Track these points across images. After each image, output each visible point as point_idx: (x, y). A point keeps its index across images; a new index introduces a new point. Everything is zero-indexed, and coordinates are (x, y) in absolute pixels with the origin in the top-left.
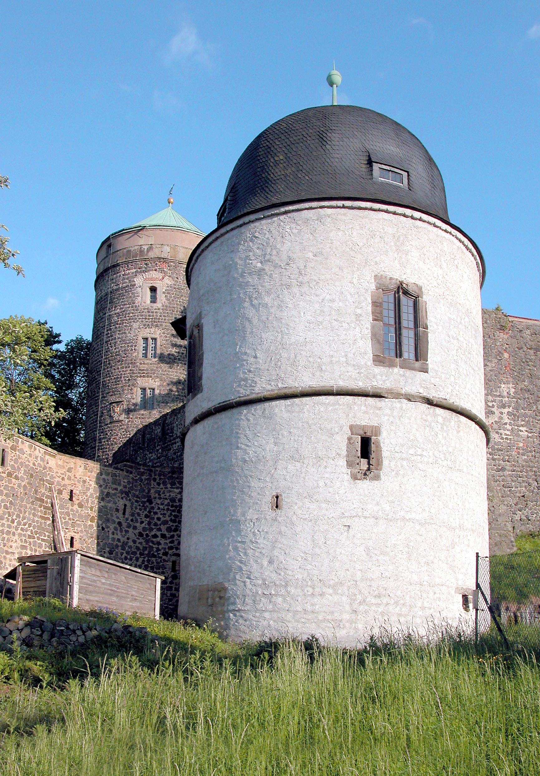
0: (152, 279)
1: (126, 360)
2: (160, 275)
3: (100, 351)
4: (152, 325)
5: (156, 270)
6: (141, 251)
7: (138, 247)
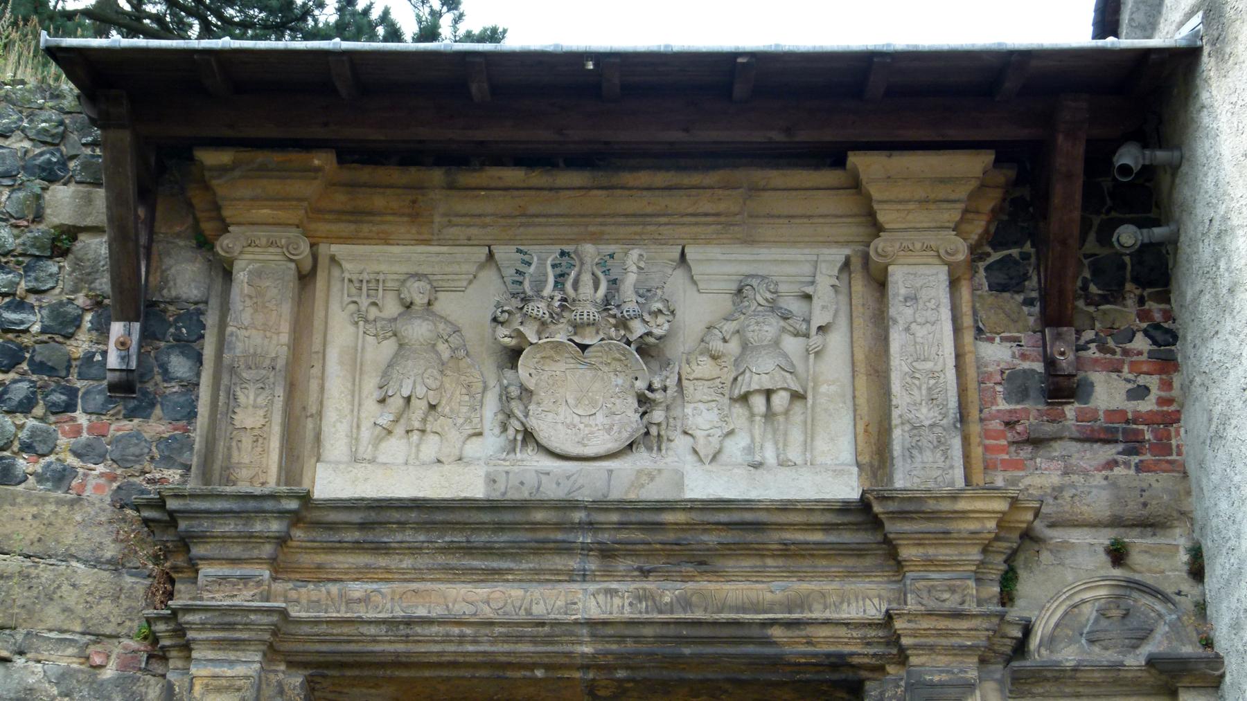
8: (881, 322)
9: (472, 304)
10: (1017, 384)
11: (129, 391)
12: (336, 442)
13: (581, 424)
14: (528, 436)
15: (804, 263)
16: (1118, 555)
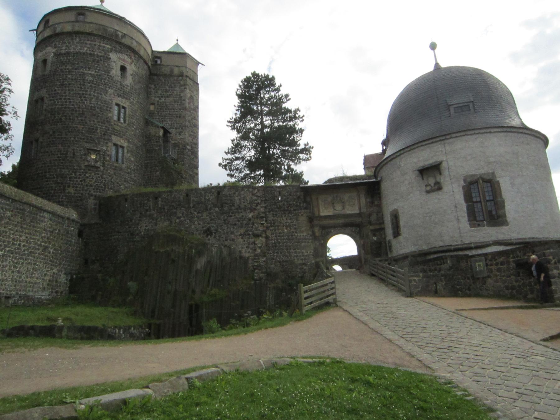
0: (124, 60)
2: (129, 60)
3: (69, 99)
5: (127, 55)
6: (117, 36)
8: (360, 199)
9: (330, 199)
11: (306, 208)
12: (321, 211)
13: (339, 208)
15: (354, 194)
16: (377, 215)
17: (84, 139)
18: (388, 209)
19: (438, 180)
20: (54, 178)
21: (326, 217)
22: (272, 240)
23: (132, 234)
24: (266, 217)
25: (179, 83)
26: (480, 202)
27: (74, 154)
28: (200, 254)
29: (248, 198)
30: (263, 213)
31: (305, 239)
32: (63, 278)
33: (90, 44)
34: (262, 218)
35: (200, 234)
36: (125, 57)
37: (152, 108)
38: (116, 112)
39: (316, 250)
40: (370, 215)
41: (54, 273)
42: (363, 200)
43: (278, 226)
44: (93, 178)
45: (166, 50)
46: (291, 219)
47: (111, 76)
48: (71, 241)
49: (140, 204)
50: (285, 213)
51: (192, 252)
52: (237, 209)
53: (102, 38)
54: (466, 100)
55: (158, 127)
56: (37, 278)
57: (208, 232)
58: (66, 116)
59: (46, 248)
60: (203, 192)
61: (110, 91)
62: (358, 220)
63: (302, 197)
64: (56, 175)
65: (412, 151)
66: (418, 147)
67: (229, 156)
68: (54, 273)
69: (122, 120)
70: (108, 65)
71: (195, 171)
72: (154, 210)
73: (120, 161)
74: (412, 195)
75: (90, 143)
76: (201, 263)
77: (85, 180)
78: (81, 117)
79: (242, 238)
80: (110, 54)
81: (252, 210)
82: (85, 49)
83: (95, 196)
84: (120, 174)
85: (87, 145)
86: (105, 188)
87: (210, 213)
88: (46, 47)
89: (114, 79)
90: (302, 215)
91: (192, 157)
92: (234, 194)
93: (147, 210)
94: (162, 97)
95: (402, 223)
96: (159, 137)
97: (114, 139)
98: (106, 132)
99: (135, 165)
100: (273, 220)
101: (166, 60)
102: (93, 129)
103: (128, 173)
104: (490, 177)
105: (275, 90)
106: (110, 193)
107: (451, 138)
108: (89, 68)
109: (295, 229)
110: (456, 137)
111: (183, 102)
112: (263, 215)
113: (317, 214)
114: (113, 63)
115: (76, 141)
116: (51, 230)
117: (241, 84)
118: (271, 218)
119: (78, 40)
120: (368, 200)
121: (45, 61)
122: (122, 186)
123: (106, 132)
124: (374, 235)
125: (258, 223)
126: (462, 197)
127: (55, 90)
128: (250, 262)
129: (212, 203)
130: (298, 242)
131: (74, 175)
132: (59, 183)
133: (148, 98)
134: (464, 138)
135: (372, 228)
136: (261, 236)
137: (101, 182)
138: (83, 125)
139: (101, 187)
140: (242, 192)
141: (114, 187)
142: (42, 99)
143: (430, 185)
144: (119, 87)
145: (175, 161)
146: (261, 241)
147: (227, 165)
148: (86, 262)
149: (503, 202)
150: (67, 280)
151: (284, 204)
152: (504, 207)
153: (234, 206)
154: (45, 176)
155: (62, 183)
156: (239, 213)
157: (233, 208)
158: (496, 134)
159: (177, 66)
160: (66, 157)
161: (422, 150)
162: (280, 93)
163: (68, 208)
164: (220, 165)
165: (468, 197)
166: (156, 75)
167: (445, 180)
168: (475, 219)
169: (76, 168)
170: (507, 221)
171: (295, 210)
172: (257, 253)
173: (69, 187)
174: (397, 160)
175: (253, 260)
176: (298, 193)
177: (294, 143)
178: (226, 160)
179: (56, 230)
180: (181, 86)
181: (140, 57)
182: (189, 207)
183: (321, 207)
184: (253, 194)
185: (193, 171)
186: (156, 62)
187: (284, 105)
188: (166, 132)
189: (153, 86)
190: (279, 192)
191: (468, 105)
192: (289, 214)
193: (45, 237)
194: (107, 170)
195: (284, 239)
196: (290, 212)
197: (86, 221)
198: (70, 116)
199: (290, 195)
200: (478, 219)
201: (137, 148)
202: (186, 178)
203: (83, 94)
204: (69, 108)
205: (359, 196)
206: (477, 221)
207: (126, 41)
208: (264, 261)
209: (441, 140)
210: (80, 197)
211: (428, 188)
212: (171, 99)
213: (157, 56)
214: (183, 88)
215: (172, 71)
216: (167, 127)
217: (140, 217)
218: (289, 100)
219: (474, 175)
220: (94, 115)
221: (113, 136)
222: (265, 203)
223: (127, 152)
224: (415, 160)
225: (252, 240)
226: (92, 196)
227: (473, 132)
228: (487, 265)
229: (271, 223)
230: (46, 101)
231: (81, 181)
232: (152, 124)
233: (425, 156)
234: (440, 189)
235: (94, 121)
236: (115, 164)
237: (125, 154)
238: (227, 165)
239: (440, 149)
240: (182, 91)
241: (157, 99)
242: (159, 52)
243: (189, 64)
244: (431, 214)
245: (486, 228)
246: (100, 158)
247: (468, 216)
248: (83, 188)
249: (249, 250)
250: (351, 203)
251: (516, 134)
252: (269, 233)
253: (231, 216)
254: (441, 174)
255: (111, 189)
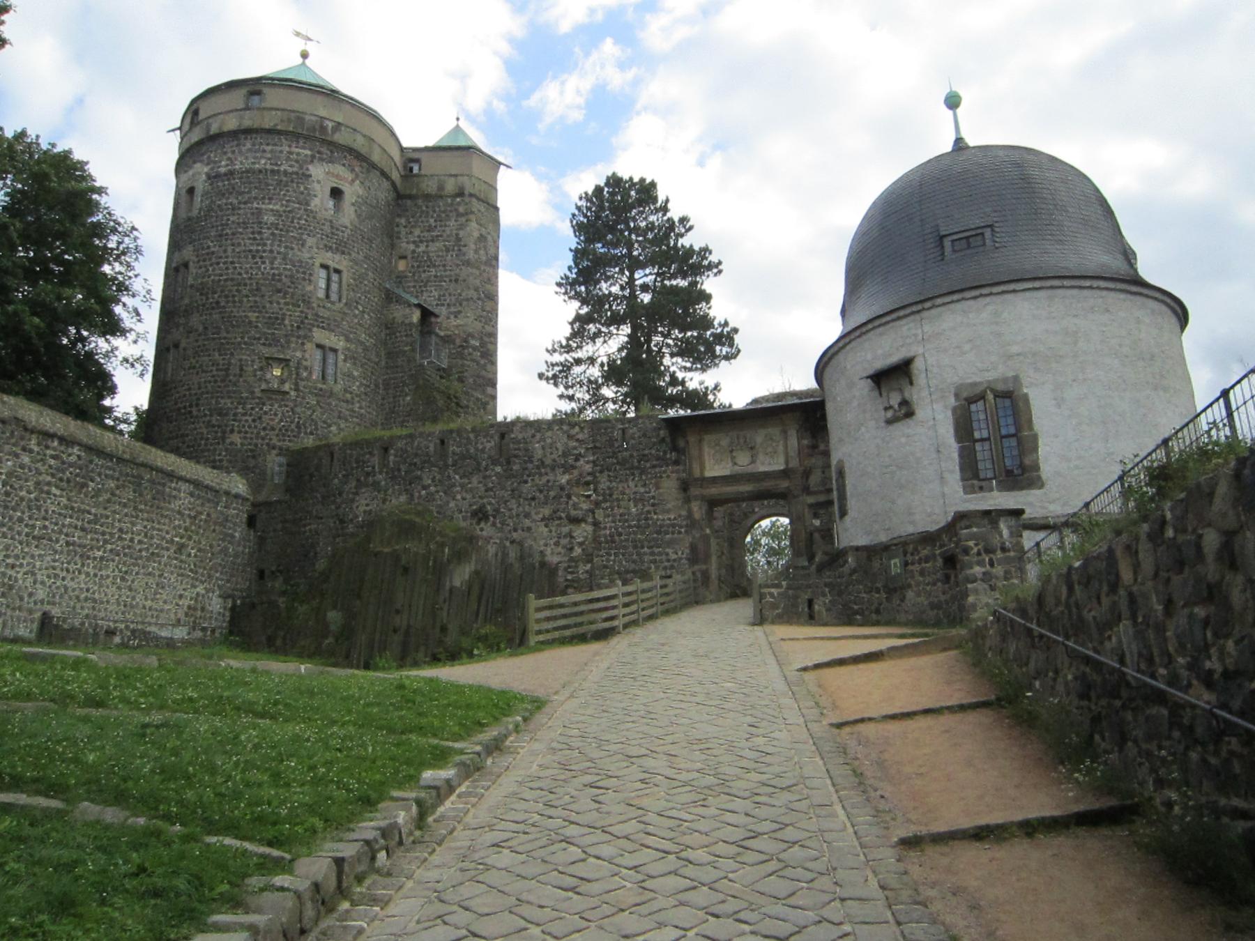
0: (337, 176)
1: (293, 294)
2: (350, 176)
3: (232, 263)
4: (337, 249)
6: (323, 129)
7: (313, 118)
8: (786, 439)
10: (808, 447)
11: (676, 462)
14: (735, 464)
15: (775, 431)
17: (259, 339)
18: (834, 462)
19: (907, 395)
20: (205, 415)
21: (714, 480)
22: (605, 528)
23: (342, 522)
24: (596, 483)
25: (456, 210)
26: (989, 439)
27: (241, 370)
28: (460, 556)
29: (559, 445)
30: (589, 474)
31: (673, 526)
32: (216, 604)
33: (272, 151)
34: (588, 484)
35: (465, 519)
36: (339, 169)
37: (402, 265)
38: (322, 284)
39: (693, 548)
40: (807, 473)
41: (198, 594)
42: (793, 442)
43: (618, 500)
44: (276, 415)
45: (430, 144)
46: (645, 485)
47: (312, 211)
48: (233, 536)
49: (357, 462)
50: (633, 474)
51: (443, 552)
52: (538, 467)
53: (294, 136)
54: (979, 223)
55: (409, 305)
56: (165, 602)
57: (480, 515)
58: (227, 296)
59: (181, 547)
60: (472, 436)
61: (310, 241)
62: (784, 484)
63: (668, 440)
64: (210, 410)
65: (864, 337)
66: (874, 328)
67: (557, 358)
68: (198, 594)
69: (334, 297)
70: (306, 188)
71: (489, 390)
72: (381, 473)
73: (330, 379)
74: (863, 429)
75: (270, 345)
76: (461, 576)
77: (260, 418)
78: (255, 295)
79: (546, 526)
80: (310, 167)
81: (567, 469)
82: (263, 161)
83: (281, 449)
84: (330, 404)
85: (267, 351)
86: (299, 433)
87: (485, 477)
88: (195, 162)
89: (319, 216)
90: (668, 477)
91: (482, 362)
92: (533, 436)
93: (368, 474)
94: (421, 242)
95: (849, 488)
96: (411, 324)
97: (319, 335)
98: (302, 322)
99: (361, 384)
100: (609, 488)
101: (430, 166)
102: (277, 318)
103: (347, 402)
104: (1010, 387)
105: (657, 210)
106: (309, 442)
107: (933, 307)
108: (270, 199)
109: (653, 505)
110: (944, 304)
111: (464, 249)
112: (589, 478)
113: (697, 473)
114: (315, 184)
115: (245, 343)
116: (193, 514)
117: (583, 203)
118: (604, 483)
119: (249, 145)
120: (805, 442)
121: (191, 191)
122: (333, 428)
123: (302, 322)
124: (816, 516)
125: (578, 496)
126: (952, 431)
127: (209, 247)
128: (560, 573)
129: (490, 457)
130: (659, 532)
131: (240, 410)
132: (214, 426)
133: (393, 246)
134: (958, 306)
135: (811, 500)
136: (586, 522)
137: (292, 422)
138: (260, 312)
139: (292, 431)
140: (549, 434)
141: (317, 429)
142: (186, 265)
143: (891, 407)
144: (327, 228)
145: (444, 373)
146: (583, 532)
147: (559, 375)
148: (261, 575)
149: (1035, 438)
150: (225, 608)
151: (631, 456)
152: (1035, 449)
153: (532, 462)
154: (190, 412)
155: (219, 426)
156: (541, 475)
157: (530, 466)
158: (1027, 294)
159: (451, 175)
160: (227, 375)
161: (881, 334)
162: (669, 215)
163: (228, 472)
164: (541, 376)
165: (964, 429)
166: (410, 197)
167: (919, 394)
168: (976, 476)
169: (244, 395)
170: (1039, 478)
171: (654, 467)
172: (574, 554)
173: (232, 431)
174: (841, 356)
175: (566, 569)
176: (662, 432)
177: (706, 322)
178: (553, 365)
179: (201, 513)
180: (459, 215)
181: (373, 166)
182: (446, 466)
183: (706, 458)
184: (570, 437)
185: (484, 392)
186: (411, 169)
187: (681, 241)
188: (426, 314)
189: (403, 221)
190: (623, 431)
191: (982, 234)
192: (641, 474)
193: (180, 527)
194: (304, 398)
195: (630, 526)
196: (643, 471)
197: (261, 498)
198: (234, 296)
199: (644, 435)
200: (982, 475)
201: (366, 349)
202: (467, 407)
203: (258, 251)
204: (232, 280)
205: (785, 432)
206: (980, 480)
207: (342, 138)
208: (587, 572)
209: (913, 313)
210: (251, 451)
211: (890, 414)
212: (439, 244)
213: (412, 158)
214: (463, 219)
215: (441, 187)
216: (430, 298)
217: (356, 487)
218: (691, 228)
219: (975, 384)
220: (279, 291)
221: (315, 329)
222: (594, 454)
223: (345, 361)
224: (869, 357)
225: (565, 530)
226: (274, 448)
227: (977, 293)
228: (906, 564)
229: (604, 495)
230: (193, 269)
231: (254, 421)
232: (399, 300)
233: (882, 350)
234: (910, 414)
235: (278, 303)
236: (320, 386)
237: (340, 364)
238: (559, 375)
239: (913, 332)
240: (461, 227)
241: (412, 247)
242: (415, 150)
243: (477, 168)
244: (894, 468)
245: (995, 493)
246: (290, 374)
247: (962, 469)
248: (258, 433)
249: (560, 549)
250: (770, 449)
251: (1075, 292)
252: (599, 514)
253: (526, 482)
254: (911, 383)
255: (311, 433)
